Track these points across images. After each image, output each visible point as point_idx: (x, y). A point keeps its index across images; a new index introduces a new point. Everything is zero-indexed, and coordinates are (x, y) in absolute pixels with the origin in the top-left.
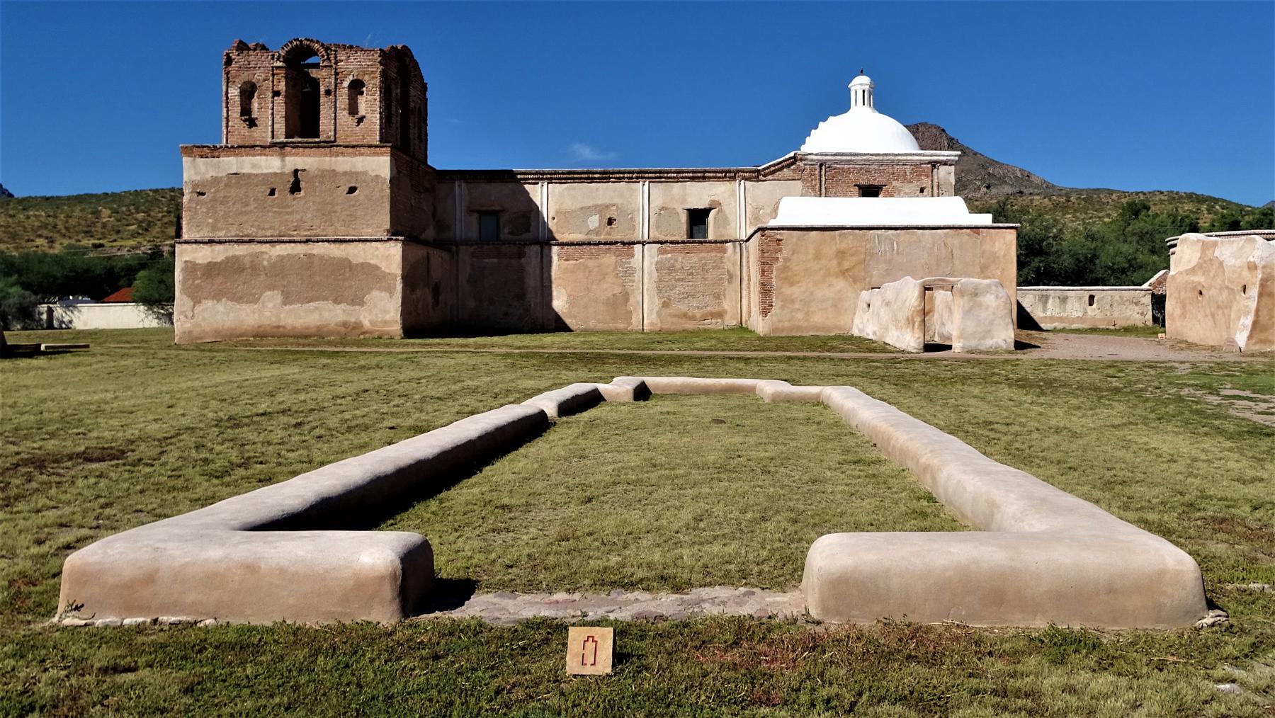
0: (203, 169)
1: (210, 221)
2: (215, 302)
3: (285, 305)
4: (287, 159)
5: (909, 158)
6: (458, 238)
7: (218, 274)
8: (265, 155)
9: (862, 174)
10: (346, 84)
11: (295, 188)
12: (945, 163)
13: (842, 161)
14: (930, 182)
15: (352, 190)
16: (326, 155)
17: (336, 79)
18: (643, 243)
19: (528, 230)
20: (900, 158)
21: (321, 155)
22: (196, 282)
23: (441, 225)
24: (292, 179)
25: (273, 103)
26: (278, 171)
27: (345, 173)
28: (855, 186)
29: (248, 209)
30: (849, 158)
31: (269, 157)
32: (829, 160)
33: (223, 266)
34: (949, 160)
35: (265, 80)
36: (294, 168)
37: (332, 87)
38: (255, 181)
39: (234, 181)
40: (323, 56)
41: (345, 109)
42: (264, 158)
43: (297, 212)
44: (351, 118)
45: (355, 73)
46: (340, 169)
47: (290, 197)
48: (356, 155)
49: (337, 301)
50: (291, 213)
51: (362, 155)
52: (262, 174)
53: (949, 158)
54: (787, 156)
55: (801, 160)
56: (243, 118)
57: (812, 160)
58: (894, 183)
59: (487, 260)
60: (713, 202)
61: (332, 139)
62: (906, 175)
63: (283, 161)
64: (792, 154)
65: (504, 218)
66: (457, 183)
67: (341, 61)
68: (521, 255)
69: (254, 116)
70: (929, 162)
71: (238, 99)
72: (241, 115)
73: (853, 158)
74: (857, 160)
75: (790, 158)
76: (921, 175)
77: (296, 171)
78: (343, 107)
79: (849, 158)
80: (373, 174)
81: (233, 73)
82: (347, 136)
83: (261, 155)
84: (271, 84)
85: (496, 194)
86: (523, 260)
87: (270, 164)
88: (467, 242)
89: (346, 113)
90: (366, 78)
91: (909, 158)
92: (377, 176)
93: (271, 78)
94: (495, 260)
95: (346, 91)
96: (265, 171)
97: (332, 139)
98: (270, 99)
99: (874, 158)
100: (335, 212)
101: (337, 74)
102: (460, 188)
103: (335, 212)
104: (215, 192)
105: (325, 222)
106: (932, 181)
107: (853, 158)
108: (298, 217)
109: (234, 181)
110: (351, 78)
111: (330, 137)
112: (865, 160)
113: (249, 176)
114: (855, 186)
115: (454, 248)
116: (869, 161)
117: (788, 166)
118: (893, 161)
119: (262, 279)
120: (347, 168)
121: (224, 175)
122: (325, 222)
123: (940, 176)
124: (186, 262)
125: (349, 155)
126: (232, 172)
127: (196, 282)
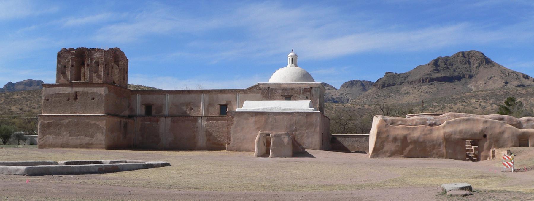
1: (50, 109)
2: (49, 135)
3: (70, 137)
6: (137, 114)
7: (51, 126)
10: (94, 62)
11: (76, 98)
15: (94, 99)
18: (201, 117)
19: (162, 112)
22: (44, 129)
23: (132, 109)
26: (70, 92)
28: (281, 96)
29: (61, 105)
33: (52, 124)
35: (69, 62)
43: (76, 106)
45: (96, 59)
46: (89, 92)
47: (74, 101)
49: (86, 136)
50: (74, 106)
58: (296, 95)
59: (146, 123)
60: (227, 101)
63: (72, 89)
65: (153, 108)
66: (138, 95)
68: (158, 121)
77: (76, 92)
85: (151, 99)
86: (159, 123)
87: (69, 90)
88: (141, 116)
94: (149, 123)
100: (87, 106)
102: (139, 97)
103: (87, 106)
104: (52, 99)
105: (84, 109)
108: (76, 108)
114: (281, 96)
115: (135, 118)
119: (63, 128)
120: (92, 91)
122: (84, 109)
124: (42, 122)
126: (57, 93)
127: (44, 129)
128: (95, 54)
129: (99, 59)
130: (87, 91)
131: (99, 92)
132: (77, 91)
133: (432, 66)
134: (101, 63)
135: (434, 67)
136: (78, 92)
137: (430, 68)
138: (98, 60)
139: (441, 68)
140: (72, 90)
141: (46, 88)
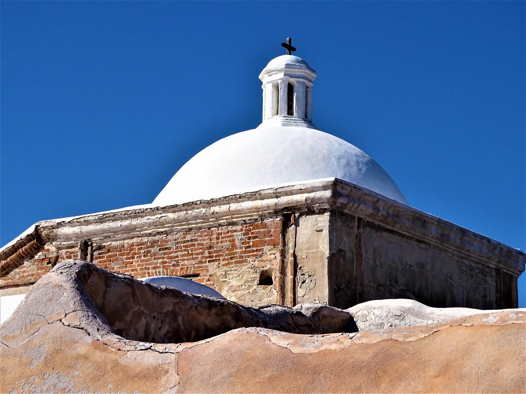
5: (234, 206)
9: (155, 254)
12: (310, 211)
13: (115, 232)
14: (279, 258)
20: (216, 209)
30: (126, 223)
32: (95, 233)
34: (313, 200)
53: (312, 195)
54: (23, 235)
55: (51, 239)
57: (67, 238)
58: (212, 268)
62: (234, 246)
64: (31, 230)
70: (276, 212)
73: (134, 222)
74: (141, 227)
75: (30, 238)
76: (264, 243)
79: (126, 223)
91: (234, 206)
99: (171, 216)
106: (283, 254)
107: (134, 222)
112: (155, 224)
116: (162, 225)
117: (30, 255)
118: (205, 218)
123: (299, 240)
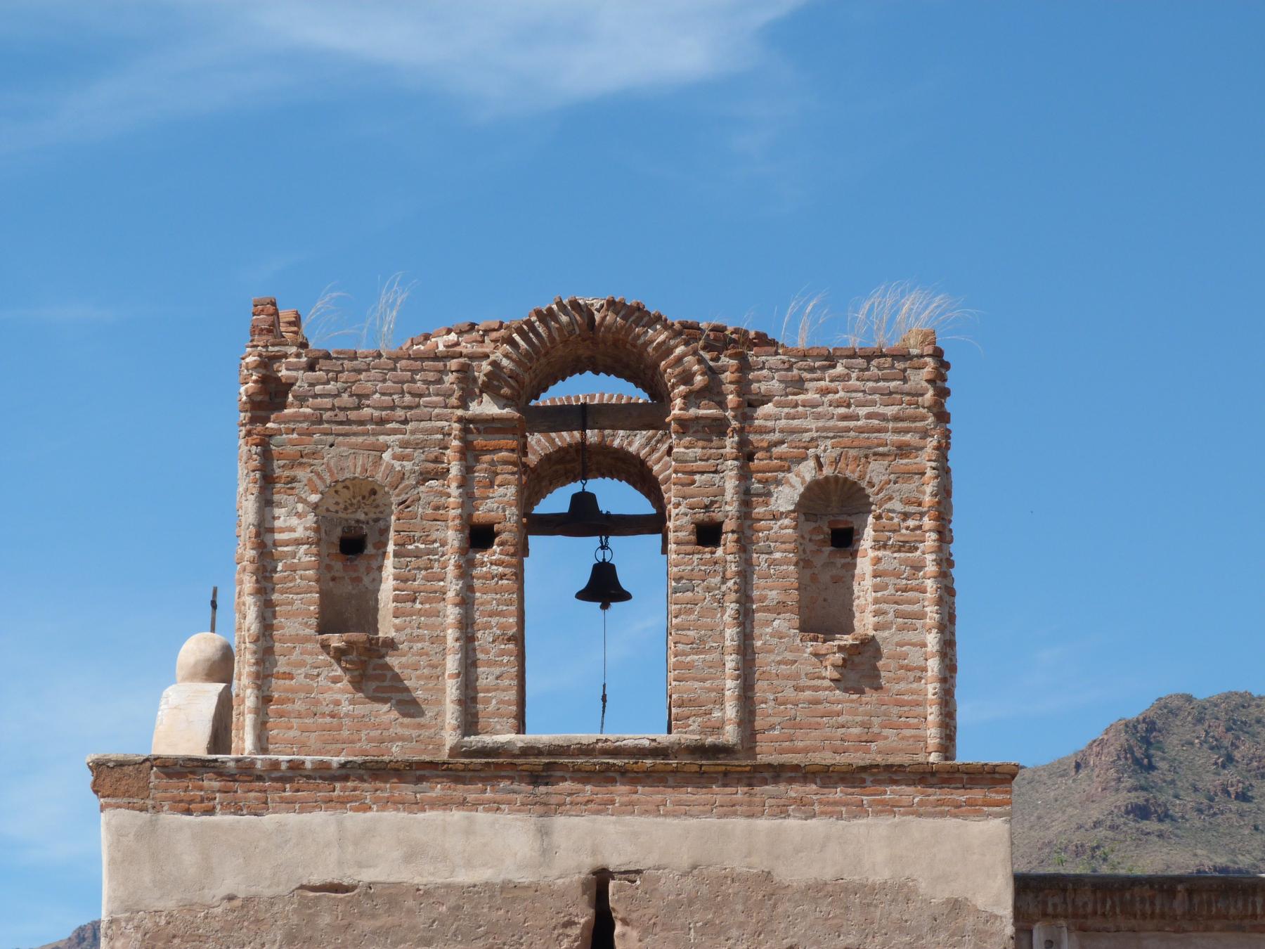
0: (189, 859)
4: (560, 822)
8: (463, 803)
10: (786, 497)
16: (730, 810)
17: (745, 475)
21: (709, 809)
24: (584, 916)
25: (465, 571)
26: (525, 878)
27: (816, 891)
31: (481, 816)
35: (425, 477)
36: (588, 863)
37: (729, 508)
38: (421, 920)
39: (325, 920)
40: (687, 378)
41: (780, 608)
42: (457, 815)
44: (810, 647)
45: (827, 450)
48: (859, 811)
51: (889, 808)
52: (448, 886)
56: (336, 640)
61: (730, 735)
63: (544, 832)
67: (765, 399)
69: (386, 629)
71: (305, 555)
72: (324, 627)
78: (774, 596)
80: (941, 894)
81: (287, 442)
82: (793, 723)
83: (444, 804)
84: (454, 490)
89: (785, 623)
90: (877, 471)
92: (956, 906)
93: (455, 469)
95: (785, 528)
96: (464, 877)
97: (730, 735)
98: (452, 560)
101: (746, 454)
109: (325, 920)
110: (807, 471)
111: (718, 728)
113: (392, 896)
120: (824, 869)
121: (282, 890)
125: (832, 811)
126: (316, 880)
128: (811, 396)
129: (870, 454)
130: (759, 863)
131: (923, 886)
132: (614, 862)
133: (1112, 773)
134: (897, 505)
135: (1128, 782)
136: (631, 874)
137: (1091, 799)
138: (852, 474)
139: (1190, 800)
140: (547, 853)
141: (157, 809)
